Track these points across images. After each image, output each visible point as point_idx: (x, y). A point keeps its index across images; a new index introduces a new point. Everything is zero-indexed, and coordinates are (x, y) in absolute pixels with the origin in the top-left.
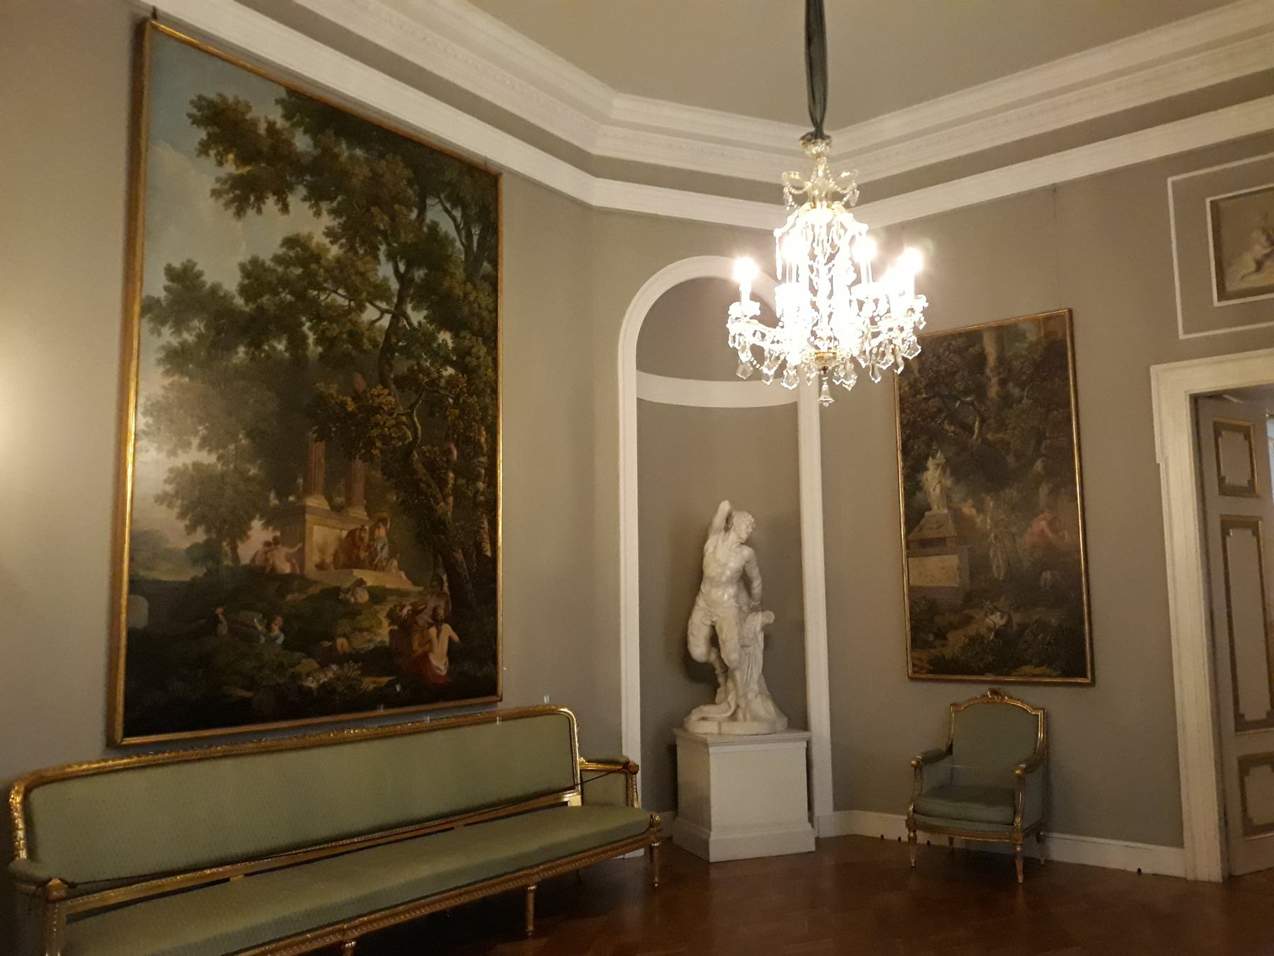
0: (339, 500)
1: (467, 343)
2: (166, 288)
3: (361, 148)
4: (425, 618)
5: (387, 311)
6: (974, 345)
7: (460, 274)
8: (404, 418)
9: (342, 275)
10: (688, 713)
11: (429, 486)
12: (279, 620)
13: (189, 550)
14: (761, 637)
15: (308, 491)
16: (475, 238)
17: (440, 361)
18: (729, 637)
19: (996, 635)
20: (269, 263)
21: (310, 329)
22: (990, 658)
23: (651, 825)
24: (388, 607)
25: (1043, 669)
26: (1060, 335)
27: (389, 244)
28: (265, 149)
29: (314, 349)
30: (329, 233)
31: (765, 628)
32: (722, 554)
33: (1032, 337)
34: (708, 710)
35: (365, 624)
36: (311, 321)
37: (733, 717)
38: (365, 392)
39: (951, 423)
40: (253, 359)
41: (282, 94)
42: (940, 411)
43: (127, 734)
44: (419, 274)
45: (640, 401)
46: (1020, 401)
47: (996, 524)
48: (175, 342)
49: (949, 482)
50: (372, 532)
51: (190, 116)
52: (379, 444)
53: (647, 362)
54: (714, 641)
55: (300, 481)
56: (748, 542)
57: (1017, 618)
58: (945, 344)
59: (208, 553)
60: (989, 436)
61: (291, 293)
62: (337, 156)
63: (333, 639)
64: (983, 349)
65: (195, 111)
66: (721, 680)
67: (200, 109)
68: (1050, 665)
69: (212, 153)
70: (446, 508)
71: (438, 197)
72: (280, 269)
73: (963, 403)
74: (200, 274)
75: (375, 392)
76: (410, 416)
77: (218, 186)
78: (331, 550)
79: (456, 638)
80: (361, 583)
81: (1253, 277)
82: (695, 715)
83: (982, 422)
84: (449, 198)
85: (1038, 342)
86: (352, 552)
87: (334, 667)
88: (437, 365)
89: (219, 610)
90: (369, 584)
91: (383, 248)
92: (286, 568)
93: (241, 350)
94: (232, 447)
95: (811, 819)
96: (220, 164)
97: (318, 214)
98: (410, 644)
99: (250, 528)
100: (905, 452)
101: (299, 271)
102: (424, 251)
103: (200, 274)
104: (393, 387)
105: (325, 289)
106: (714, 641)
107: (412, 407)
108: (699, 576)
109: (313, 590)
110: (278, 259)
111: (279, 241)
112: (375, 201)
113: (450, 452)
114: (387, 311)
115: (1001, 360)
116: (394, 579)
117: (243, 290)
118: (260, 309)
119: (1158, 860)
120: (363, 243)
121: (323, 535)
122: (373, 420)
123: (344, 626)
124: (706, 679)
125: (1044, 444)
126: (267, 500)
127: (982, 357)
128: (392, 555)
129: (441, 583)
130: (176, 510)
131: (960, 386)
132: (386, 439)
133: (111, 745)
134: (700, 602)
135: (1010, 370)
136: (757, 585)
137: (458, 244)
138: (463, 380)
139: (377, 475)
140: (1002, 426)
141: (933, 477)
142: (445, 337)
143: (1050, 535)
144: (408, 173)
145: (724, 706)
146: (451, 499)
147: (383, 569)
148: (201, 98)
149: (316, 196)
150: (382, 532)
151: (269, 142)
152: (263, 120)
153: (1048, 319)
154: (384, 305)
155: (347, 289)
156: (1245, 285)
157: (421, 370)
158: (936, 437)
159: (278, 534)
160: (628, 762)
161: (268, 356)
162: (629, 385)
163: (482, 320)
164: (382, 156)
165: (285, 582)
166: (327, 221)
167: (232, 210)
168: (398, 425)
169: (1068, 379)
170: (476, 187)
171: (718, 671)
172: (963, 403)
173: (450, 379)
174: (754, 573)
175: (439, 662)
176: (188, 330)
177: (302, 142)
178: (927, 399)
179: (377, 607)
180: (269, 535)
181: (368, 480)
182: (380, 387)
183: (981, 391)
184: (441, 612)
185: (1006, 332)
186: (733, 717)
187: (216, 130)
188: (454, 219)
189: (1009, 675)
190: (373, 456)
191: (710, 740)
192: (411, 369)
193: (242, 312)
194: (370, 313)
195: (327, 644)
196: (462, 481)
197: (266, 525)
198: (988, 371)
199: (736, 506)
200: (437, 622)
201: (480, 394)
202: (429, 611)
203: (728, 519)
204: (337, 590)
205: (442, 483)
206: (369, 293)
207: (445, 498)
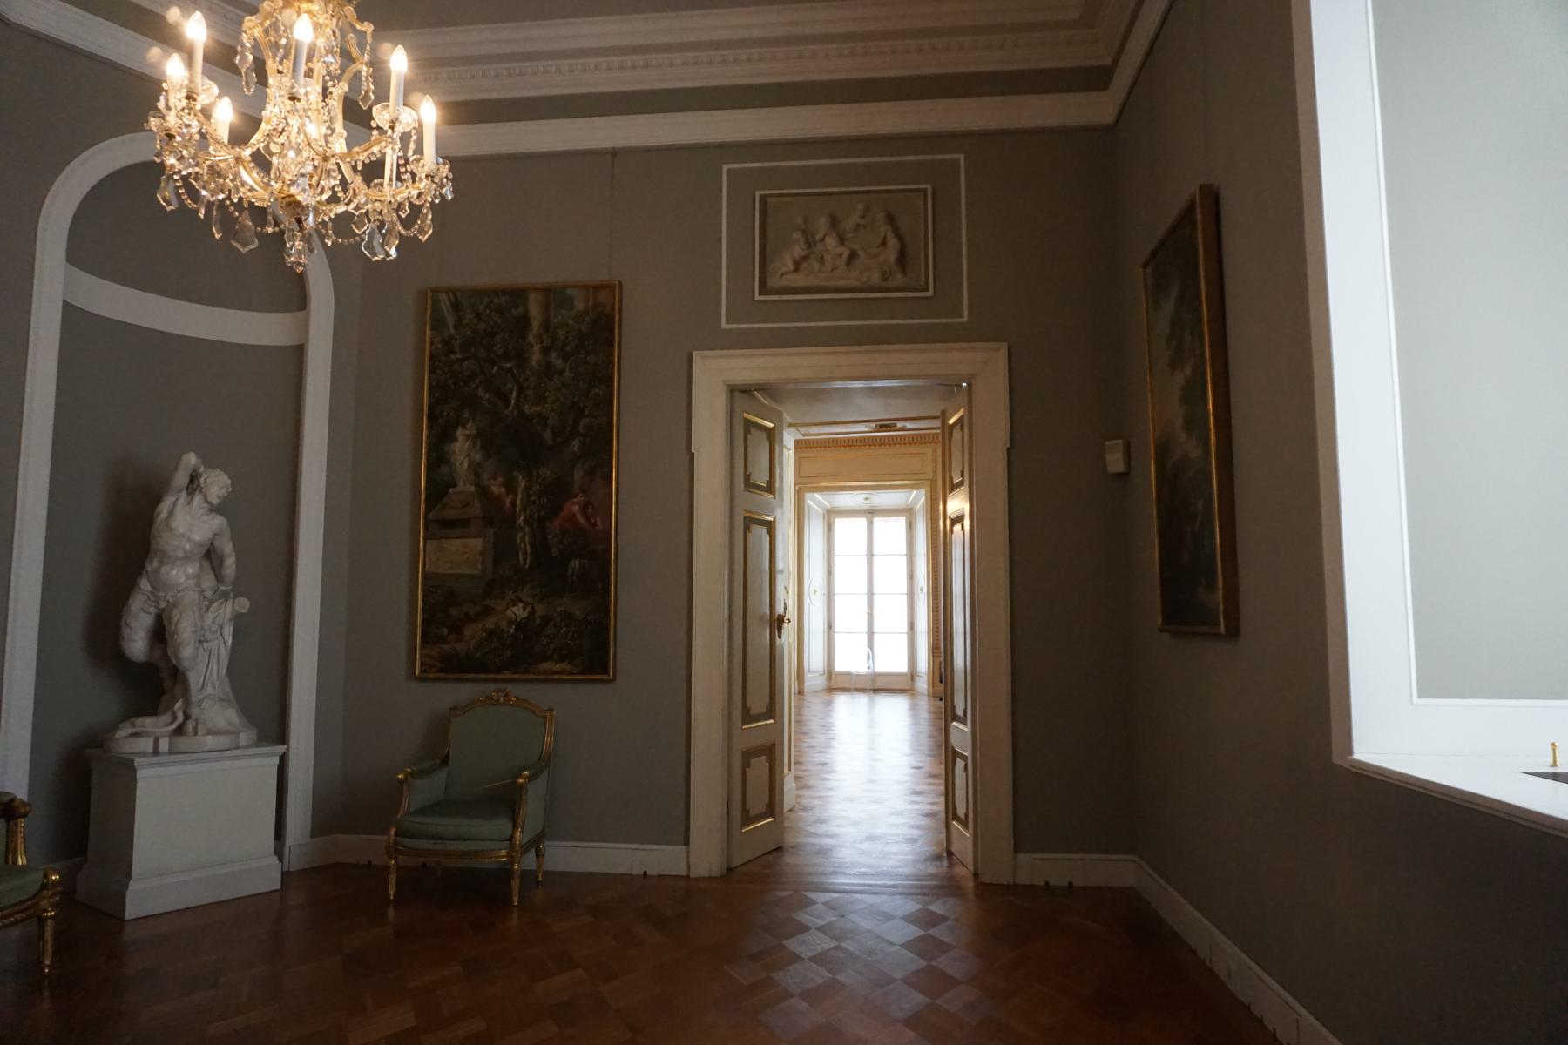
6: (517, 306)
10: (115, 727)
14: (228, 631)
18: (185, 629)
22: (509, 653)
31: (237, 618)
32: (181, 522)
33: (580, 306)
34: (148, 722)
37: (180, 731)
45: (67, 306)
46: (561, 373)
49: (478, 457)
53: (80, 253)
54: (161, 634)
57: (541, 610)
58: (487, 300)
60: (526, 409)
64: (527, 311)
66: (166, 684)
73: (501, 368)
81: (790, 277)
83: (521, 390)
85: (586, 312)
95: (279, 852)
106: (161, 634)
115: (546, 326)
119: (660, 859)
127: (524, 321)
131: (499, 350)
136: (230, 562)
141: (461, 450)
143: (582, 520)
145: (166, 717)
153: (597, 288)
156: (785, 282)
160: (13, 800)
162: (53, 280)
174: (227, 547)
183: (521, 356)
185: (553, 294)
186: (180, 731)
189: (527, 672)
198: (530, 338)
203: (194, 478)
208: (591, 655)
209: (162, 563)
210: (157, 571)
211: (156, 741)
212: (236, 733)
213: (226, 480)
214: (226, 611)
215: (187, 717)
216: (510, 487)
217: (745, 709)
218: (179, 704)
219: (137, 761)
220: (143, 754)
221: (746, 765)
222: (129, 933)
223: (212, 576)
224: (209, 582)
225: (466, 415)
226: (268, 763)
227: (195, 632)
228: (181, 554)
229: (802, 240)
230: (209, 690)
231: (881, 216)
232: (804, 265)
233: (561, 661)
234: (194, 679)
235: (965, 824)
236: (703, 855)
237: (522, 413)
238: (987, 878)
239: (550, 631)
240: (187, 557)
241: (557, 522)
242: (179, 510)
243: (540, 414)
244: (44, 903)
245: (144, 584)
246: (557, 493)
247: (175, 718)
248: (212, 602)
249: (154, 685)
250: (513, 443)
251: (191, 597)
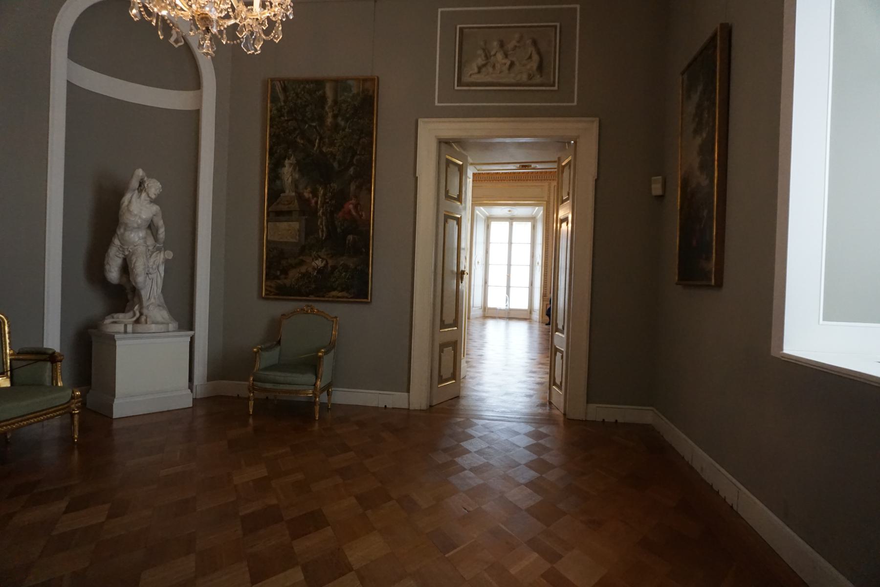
10: (103, 319)
14: (162, 269)
18: (139, 266)
22: (313, 286)
25: (344, 294)
31: (166, 262)
33: (355, 91)
34: (121, 316)
37: (137, 321)
42: (295, 129)
45: (70, 85)
46: (344, 130)
47: (324, 203)
49: (297, 176)
54: (126, 269)
57: (331, 263)
60: (324, 149)
64: (324, 93)
66: (129, 297)
73: (310, 126)
82: (108, 321)
83: (321, 139)
95: (191, 387)
115: (335, 102)
119: (395, 399)
127: (323, 98)
140: (332, 144)
141: (288, 172)
143: (354, 213)
145: (131, 314)
153: (365, 80)
162: (62, 70)
178: (288, 121)
183: (321, 119)
185: (340, 84)
186: (137, 321)
189: (323, 297)
203: (141, 183)
208: (358, 288)
209: (125, 230)
210: (123, 234)
211: (126, 326)
212: (168, 324)
213: (159, 185)
214: (160, 257)
215: (141, 314)
216: (315, 193)
217: (442, 321)
218: (136, 307)
219: (116, 336)
220: (119, 333)
221: (441, 351)
222: (115, 425)
223: (152, 238)
224: (151, 241)
226: (183, 340)
227: (144, 269)
228: (136, 225)
230: (152, 300)
231: (529, 42)
232: (484, 70)
234: (144, 294)
235: (560, 387)
237: (321, 152)
238: (571, 416)
240: (139, 228)
241: (340, 214)
242: (134, 200)
245: (117, 242)
246: (341, 198)
247: (134, 315)
248: (153, 253)
249: (123, 296)
250: (316, 169)
251: (141, 249)
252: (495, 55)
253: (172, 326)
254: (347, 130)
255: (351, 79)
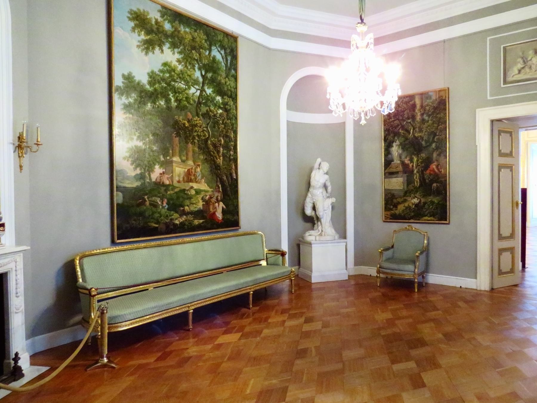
0: (184, 158)
1: (226, 100)
2: (123, 82)
3: (188, 28)
4: (214, 200)
5: (199, 89)
6: (411, 101)
7: (224, 75)
8: (205, 129)
9: (181, 76)
10: (305, 233)
11: (214, 153)
12: (166, 200)
13: (135, 176)
15: (173, 155)
16: (229, 61)
17: (217, 107)
19: (415, 206)
20: (158, 73)
21: (172, 96)
22: (413, 214)
23: (291, 272)
24: (201, 196)
25: (432, 218)
26: (444, 97)
27: (199, 64)
28: (155, 29)
29: (174, 104)
30: (179, 61)
33: (434, 98)
34: (312, 232)
35: (194, 202)
36: (172, 93)
37: (321, 235)
38: (191, 119)
39: (402, 130)
40: (153, 108)
41: (159, 8)
42: (398, 125)
43: (118, 239)
44: (209, 75)
46: (428, 121)
47: (417, 165)
48: (127, 102)
49: (400, 151)
50: (195, 170)
51: (128, 17)
52: (197, 138)
53: (291, 106)
54: (314, 208)
55: (171, 151)
56: (327, 173)
57: (423, 200)
59: (141, 177)
61: (166, 83)
62: (179, 32)
63: (183, 207)
64: (415, 102)
65: (129, 15)
66: (316, 222)
67: (131, 14)
68: (434, 217)
69: (136, 31)
70: (220, 161)
71: (216, 46)
72: (161, 75)
73: (407, 122)
74: (134, 77)
75: (195, 119)
76: (207, 127)
77: (139, 44)
78: (182, 176)
79: (224, 207)
80: (192, 187)
82: (307, 234)
83: (414, 129)
84: (220, 46)
85: (436, 100)
86: (189, 177)
87: (185, 217)
88: (216, 109)
89: (146, 197)
90: (195, 188)
91: (197, 66)
92: (167, 182)
93: (149, 104)
94: (147, 139)
95: (346, 269)
96: (139, 35)
97: (174, 53)
98: (209, 209)
99: (155, 168)
100: (385, 140)
101: (168, 75)
102: (211, 67)
103: (134, 77)
104: (201, 117)
105: (177, 82)
106: (314, 208)
107: (208, 124)
108: (309, 185)
109: (176, 190)
110: (161, 71)
111: (161, 65)
112: (194, 48)
113: (221, 140)
114: (199, 89)
115: (422, 106)
116: (203, 186)
117: (150, 83)
118: (155, 90)
120: (190, 64)
121: (179, 170)
122: (194, 130)
123: (187, 202)
124: (312, 221)
125: (436, 138)
126: (160, 158)
127: (414, 106)
128: (202, 178)
129: (219, 188)
130: (130, 162)
131: (406, 116)
132: (199, 136)
133: (113, 243)
134: (309, 195)
135: (425, 110)
137: (223, 64)
138: (225, 114)
139: (196, 149)
140: (421, 131)
141: (395, 150)
142: (219, 98)
143: (436, 170)
144: (205, 37)
145: (317, 231)
146: (221, 158)
147: (199, 183)
148: (131, 10)
149: (174, 46)
150: (199, 170)
151: (156, 26)
152: (153, 18)
153: (440, 91)
154: (197, 87)
155: (185, 81)
157: (211, 111)
158: (397, 134)
159: (164, 170)
161: (158, 107)
162: (285, 115)
163: (231, 91)
164: (195, 31)
165: (167, 187)
166: (177, 56)
167: (144, 52)
168: (203, 131)
169: (446, 114)
170: (229, 43)
171: (315, 219)
172: (407, 122)
173: (221, 115)
174: (328, 184)
175: (219, 215)
176: (131, 97)
177: (167, 26)
178: (394, 121)
179: (198, 196)
180: (161, 171)
181: (194, 151)
182: (197, 117)
183: (413, 117)
184: (219, 198)
185: (424, 95)
186: (321, 235)
187: (137, 22)
188: (221, 54)
189: (419, 220)
190: (195, 142)
191: (312, 242)
192: (207, 111)
193: (149, 91)
194: (192, 90)
195: (182, 209)
196: (225, 151)
197: (160, 167)
198: (417, 111)
199: (323, 160)
200: (218, 201)
201: (230, 119)
202: (215, 198)
204: (184, 190)
205: (218, 152)
206: (192, 83)
207: (219, 157)
208: (441, 214)
215: (322, 231)
216: (411, 160)
217: (500, 234)
221: (500, 254)
222: (313, 286)
225: (396, 138)
229: (521, 61)
232: (523, 71)
233: (431, 216)
236: (482, 282)
237: (414, 136)
239: (426, 206)
241: (428, 172)
243: (421, 136)
244: (292, 276)
246: (428, 162)
250: (413, 146)
252: (531, 60)
253: (337, 237)
254: (430, 122)
255: (431, 92)
